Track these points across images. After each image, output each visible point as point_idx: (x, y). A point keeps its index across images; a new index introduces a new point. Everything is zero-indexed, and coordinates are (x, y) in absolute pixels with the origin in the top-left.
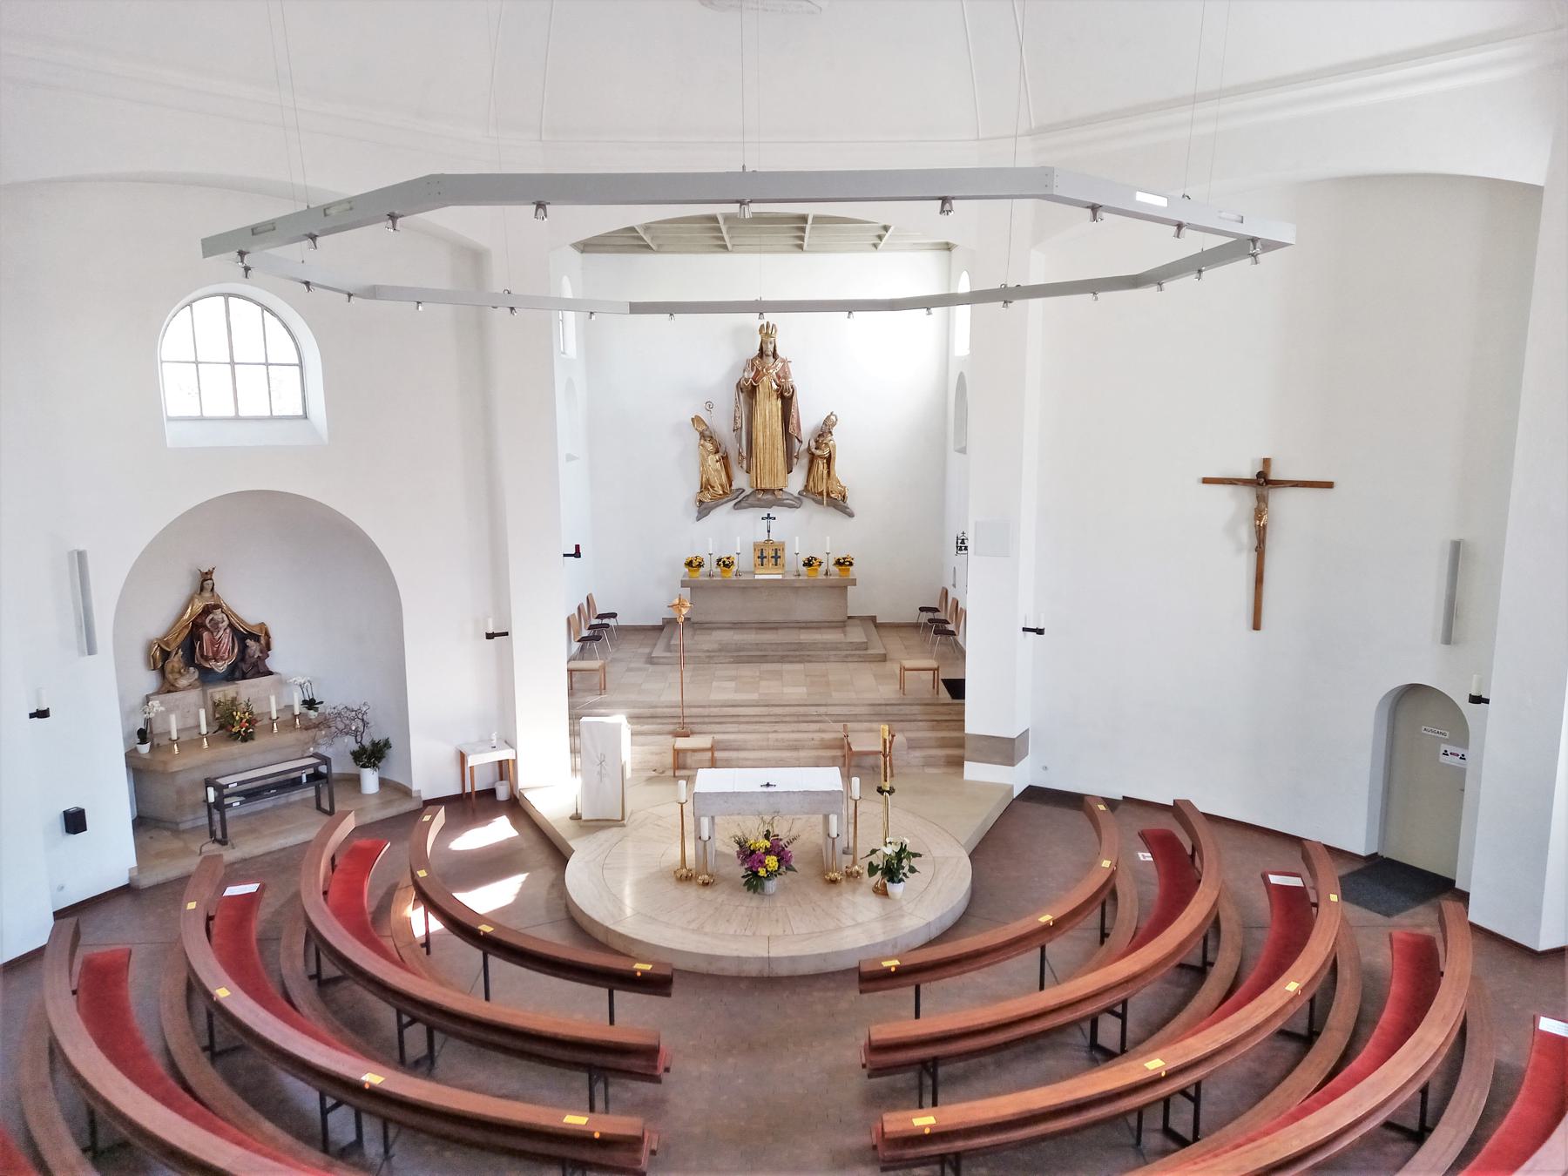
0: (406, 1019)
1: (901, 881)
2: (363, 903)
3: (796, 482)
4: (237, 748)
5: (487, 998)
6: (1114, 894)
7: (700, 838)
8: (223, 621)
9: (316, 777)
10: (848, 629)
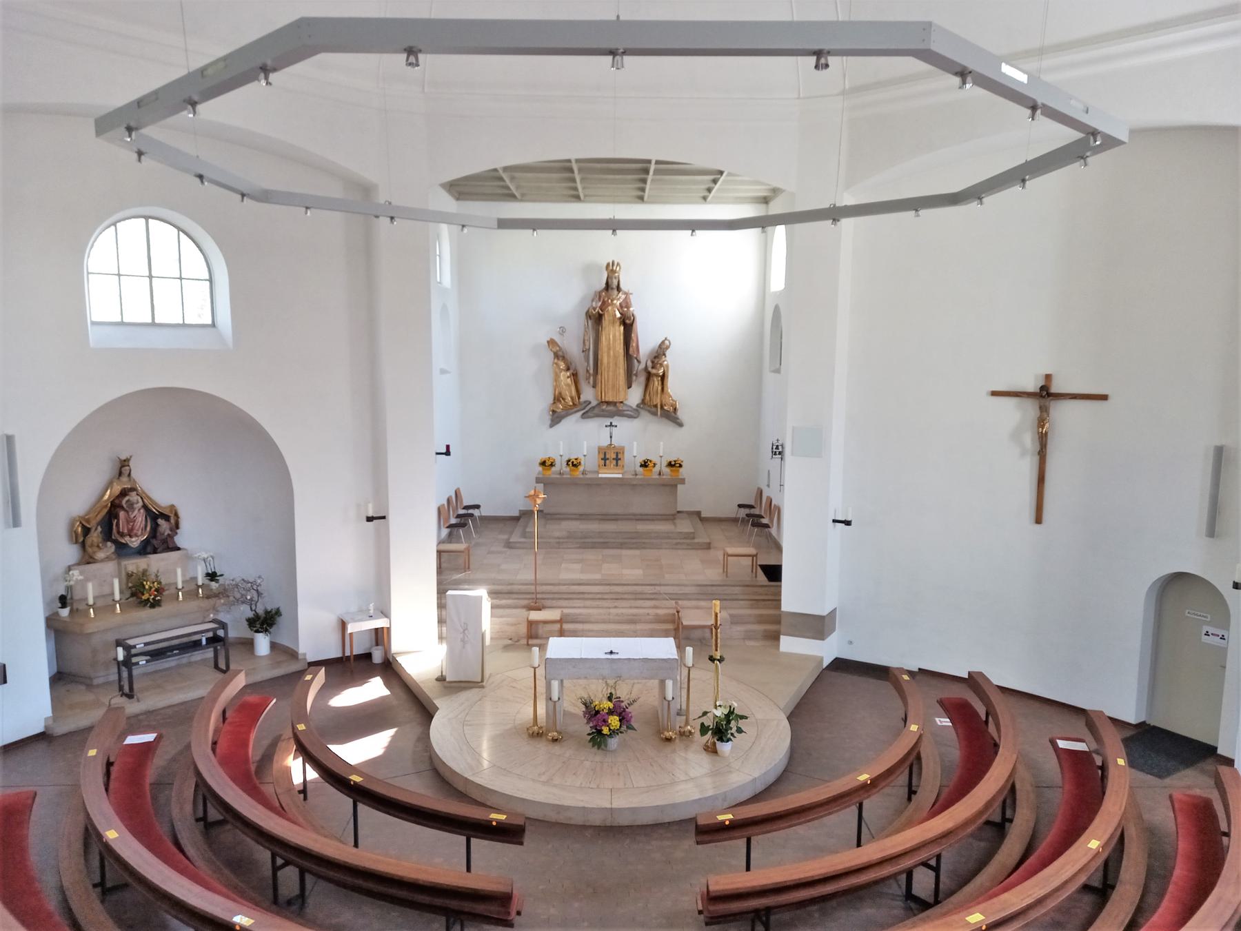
0: (279, 861)
1: (728, 741)
2: (247, 753)
3: (634, 396)
4: (147, 613)
5: (356, 845)
6: (919, 758)
7: (551, 699)
8: (138, 502)
9: (214, 640)
10: (677, 521)
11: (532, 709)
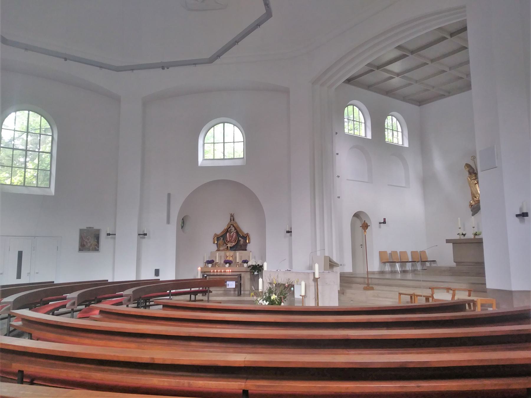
11: (43, 186)
